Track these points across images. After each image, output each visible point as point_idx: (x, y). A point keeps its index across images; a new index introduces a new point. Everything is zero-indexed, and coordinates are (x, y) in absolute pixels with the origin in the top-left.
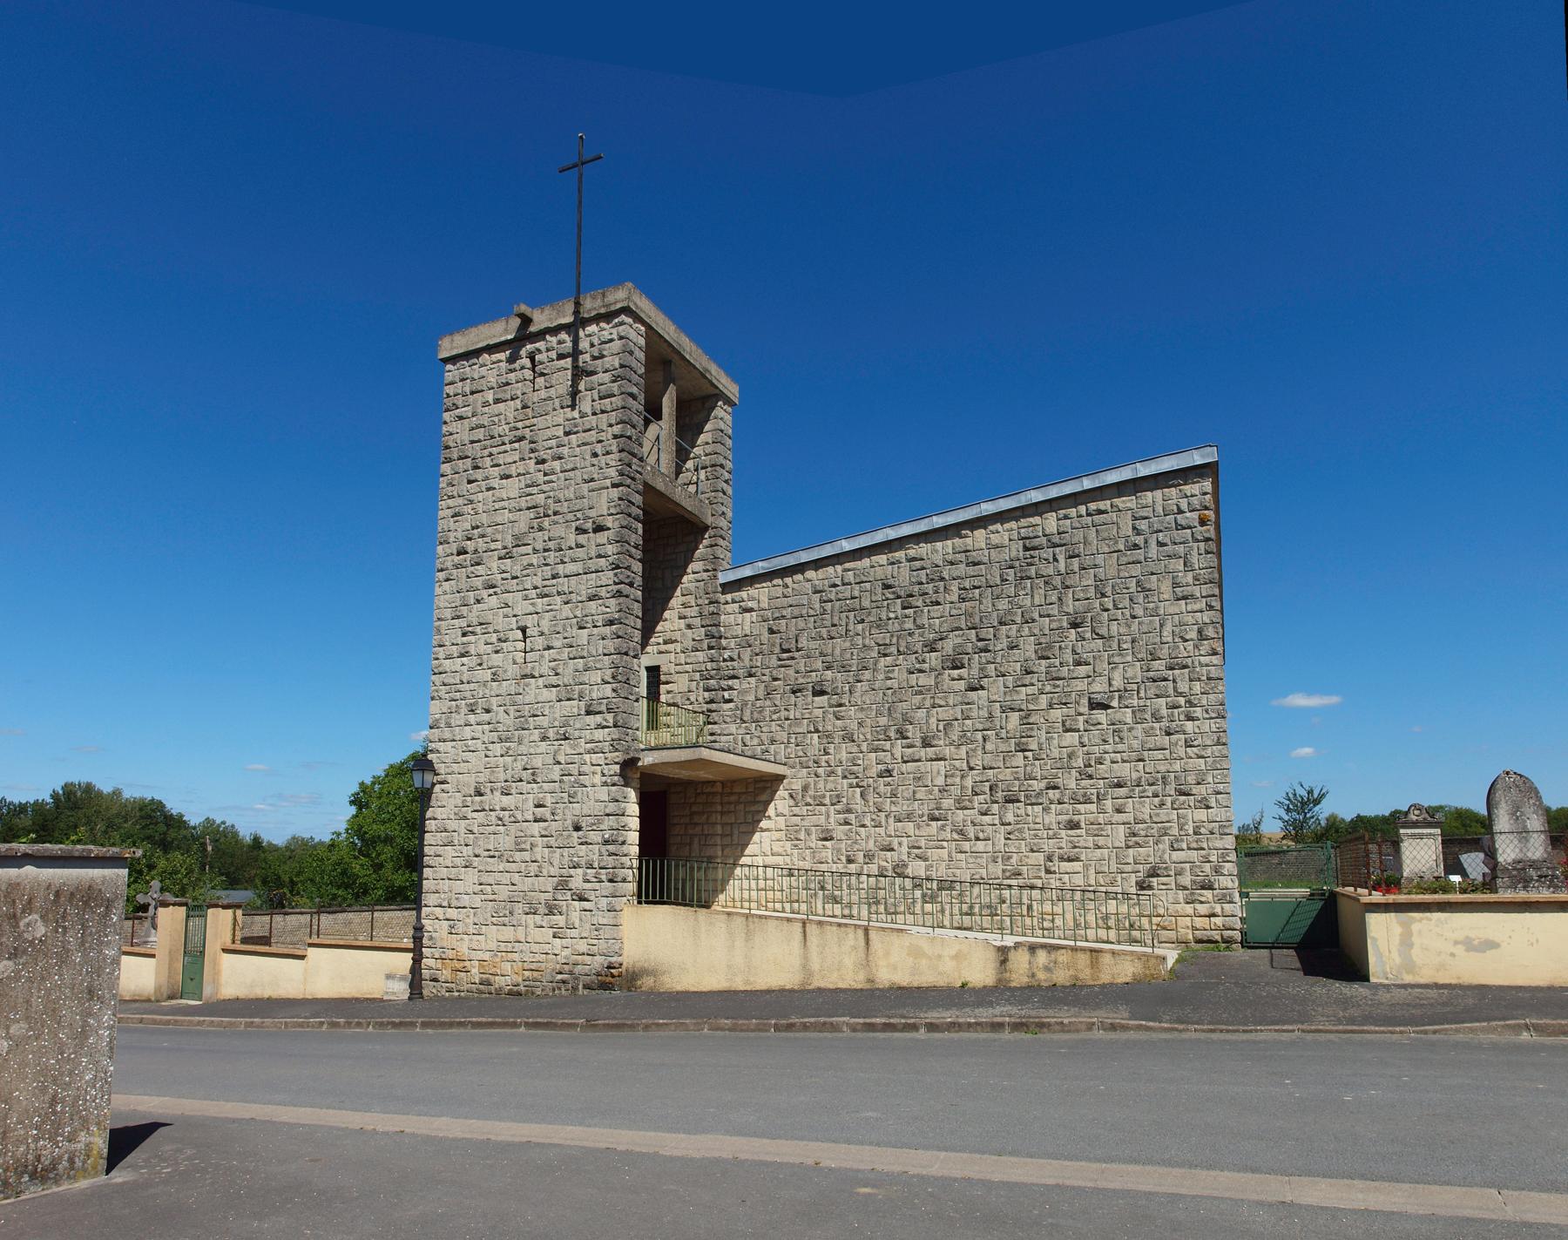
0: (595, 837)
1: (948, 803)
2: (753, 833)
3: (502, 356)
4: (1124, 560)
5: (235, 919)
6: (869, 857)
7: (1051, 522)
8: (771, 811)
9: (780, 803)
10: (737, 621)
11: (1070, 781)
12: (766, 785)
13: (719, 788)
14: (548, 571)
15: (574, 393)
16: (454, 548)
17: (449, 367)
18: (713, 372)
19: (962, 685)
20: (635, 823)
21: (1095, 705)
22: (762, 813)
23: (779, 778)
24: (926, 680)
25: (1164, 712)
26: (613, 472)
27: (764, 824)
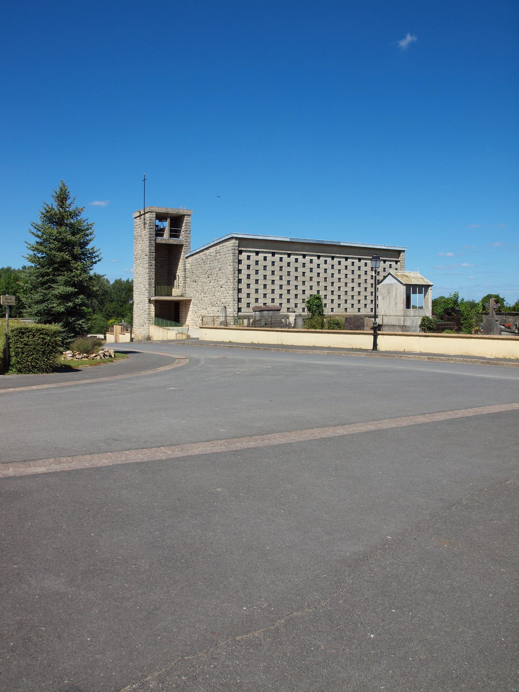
0: (147, 313)
1: (207, 306)
2: (188, 311)
3: (139, 218)
4: (225, 257)
5: (121, 328)
6: (200, 317)
7: (218, 247)
8: (190, 307)
9: (191, 306)
10: (188, 266)
11: (218, 302)
12: (190, 301)
13: (184, 302)
14: (142, 263)
15: (145, 228)
16: (134, 257)
17: (135, 220)
18: (181, 211)
19: (209, 282)
20: (154, 310)
21: (221, 287)
22: (189, 308)
23: (191, 300)
24: (205, 280)
25: (227, 289)
26: (148, 244)
27: (190, 310)
